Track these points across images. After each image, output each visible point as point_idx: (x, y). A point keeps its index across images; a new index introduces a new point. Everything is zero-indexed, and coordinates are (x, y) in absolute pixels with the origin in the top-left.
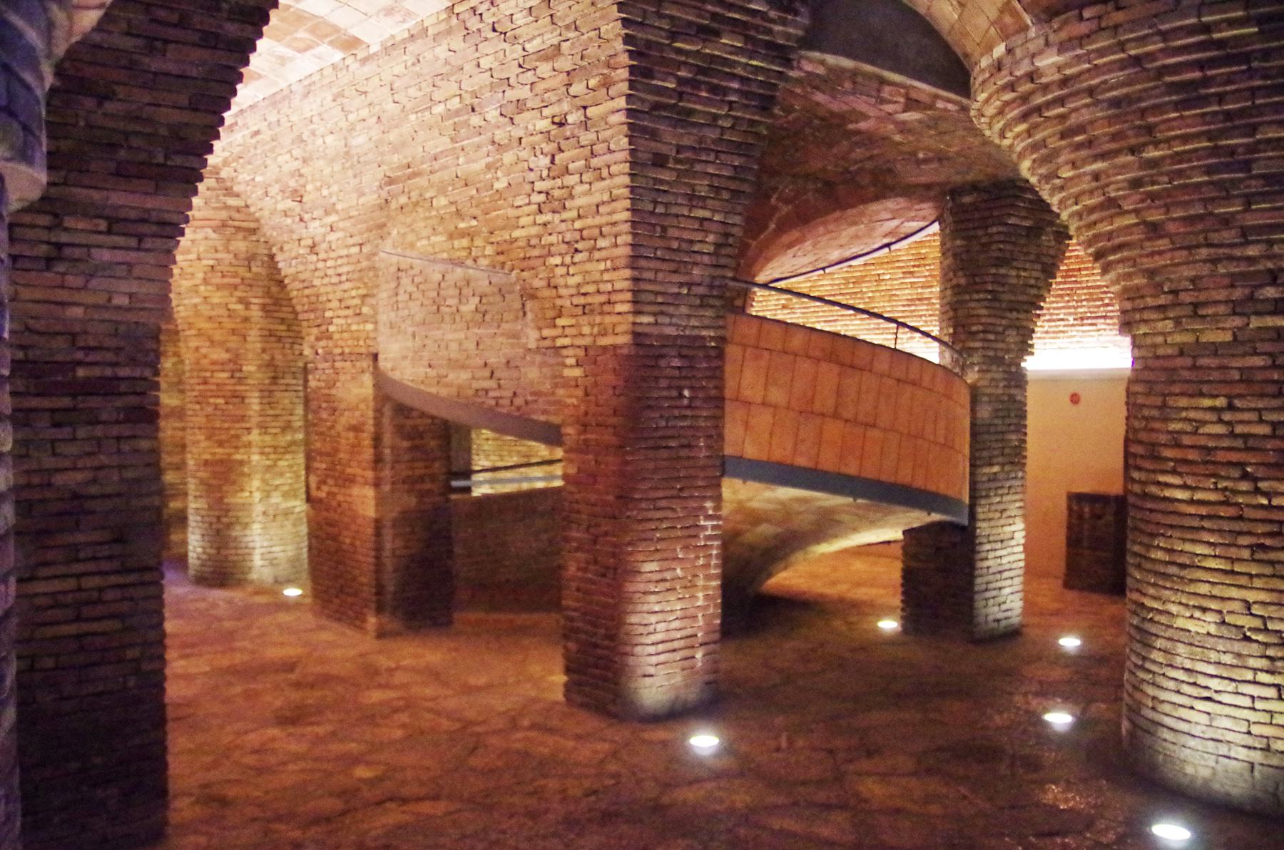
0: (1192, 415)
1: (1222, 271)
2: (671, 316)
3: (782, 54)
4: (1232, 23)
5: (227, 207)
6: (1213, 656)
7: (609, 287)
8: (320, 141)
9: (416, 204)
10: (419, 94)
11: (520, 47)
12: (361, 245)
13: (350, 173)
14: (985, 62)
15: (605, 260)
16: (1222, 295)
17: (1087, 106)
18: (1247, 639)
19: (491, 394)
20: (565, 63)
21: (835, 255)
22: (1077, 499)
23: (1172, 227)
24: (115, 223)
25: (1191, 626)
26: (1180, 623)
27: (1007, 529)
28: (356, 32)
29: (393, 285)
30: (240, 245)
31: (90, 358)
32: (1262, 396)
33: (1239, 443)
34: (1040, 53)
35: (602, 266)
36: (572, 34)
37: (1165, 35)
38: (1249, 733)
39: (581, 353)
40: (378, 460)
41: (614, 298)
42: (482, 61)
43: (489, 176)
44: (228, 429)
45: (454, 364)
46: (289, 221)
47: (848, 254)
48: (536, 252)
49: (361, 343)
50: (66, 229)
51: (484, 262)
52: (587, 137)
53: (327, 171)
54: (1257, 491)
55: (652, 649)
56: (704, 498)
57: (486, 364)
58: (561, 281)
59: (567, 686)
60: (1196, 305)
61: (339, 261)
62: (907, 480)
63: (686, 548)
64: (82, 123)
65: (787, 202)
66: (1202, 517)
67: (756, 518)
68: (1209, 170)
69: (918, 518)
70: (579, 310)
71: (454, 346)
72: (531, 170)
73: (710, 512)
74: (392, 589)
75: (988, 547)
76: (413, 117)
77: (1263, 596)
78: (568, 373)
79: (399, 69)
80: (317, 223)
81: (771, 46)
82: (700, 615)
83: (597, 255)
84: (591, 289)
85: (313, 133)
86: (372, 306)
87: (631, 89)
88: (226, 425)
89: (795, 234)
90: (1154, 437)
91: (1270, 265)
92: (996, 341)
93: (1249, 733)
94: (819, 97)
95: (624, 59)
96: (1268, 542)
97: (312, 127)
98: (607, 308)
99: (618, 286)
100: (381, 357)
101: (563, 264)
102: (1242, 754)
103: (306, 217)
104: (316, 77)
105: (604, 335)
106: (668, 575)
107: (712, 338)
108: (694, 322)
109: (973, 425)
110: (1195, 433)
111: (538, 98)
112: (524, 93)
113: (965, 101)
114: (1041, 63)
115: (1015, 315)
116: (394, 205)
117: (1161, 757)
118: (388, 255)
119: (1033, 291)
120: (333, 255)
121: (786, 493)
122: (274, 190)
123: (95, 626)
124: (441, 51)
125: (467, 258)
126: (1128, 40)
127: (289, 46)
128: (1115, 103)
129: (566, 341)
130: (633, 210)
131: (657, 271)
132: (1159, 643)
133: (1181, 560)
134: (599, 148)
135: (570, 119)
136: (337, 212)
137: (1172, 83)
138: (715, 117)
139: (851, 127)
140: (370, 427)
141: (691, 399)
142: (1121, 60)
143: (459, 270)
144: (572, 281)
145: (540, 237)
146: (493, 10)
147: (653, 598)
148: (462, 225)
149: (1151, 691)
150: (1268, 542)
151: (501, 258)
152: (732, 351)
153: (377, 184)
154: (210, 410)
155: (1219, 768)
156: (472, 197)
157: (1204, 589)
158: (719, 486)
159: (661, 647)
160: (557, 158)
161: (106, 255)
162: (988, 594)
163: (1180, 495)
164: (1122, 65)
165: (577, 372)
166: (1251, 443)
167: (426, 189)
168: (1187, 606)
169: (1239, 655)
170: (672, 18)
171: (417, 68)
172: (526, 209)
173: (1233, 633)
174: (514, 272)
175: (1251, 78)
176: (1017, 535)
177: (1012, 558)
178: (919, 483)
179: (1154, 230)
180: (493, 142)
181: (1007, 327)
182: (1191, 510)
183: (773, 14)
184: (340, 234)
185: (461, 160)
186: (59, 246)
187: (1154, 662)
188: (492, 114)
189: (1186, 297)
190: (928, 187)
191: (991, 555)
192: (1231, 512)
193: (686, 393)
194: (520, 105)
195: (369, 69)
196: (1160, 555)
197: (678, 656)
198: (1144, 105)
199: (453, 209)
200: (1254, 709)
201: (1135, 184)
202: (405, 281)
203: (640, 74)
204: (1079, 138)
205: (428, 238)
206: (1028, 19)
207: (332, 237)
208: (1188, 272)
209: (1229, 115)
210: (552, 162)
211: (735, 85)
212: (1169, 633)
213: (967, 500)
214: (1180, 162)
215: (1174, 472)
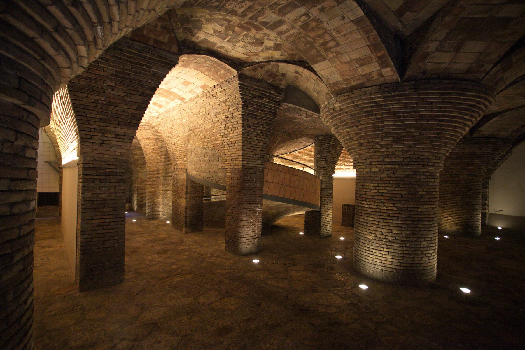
0: (370, 188)
1: (376, 154)
2: (251, 162)
3: (278, 104)
4: (378, 98)
5: (157, 136)
6: (374, 244)
8: (176, 121)
9: (196, 135)
10: (197, 110)
12: (184, 144)
13: (182, 128)
14: (323, 106)
15: (236, 148)
16: (376, 160)
17: (346, 116)
18: (381, 240)
19: (211, 179)
20: (228, 104)
21: (292, 150)
22: (345, 205)
23: (365, 144)
24: (117, 136)
25: (369, 237)
26: (366, 236)
27: (328, 212)
28: (183, 96)
29: (190, 153)
30: (160, 144)
31: (110, 167)
32: (385, 184)
33: (380, 195)
34: (335, 103)
36: (229, 97)
37: (363, 100)
38: (382, 263)
39: (231, 170)
40: (186, 193)
41: (239, 157)
42: (210, 103)
44: (156, 185)
45: (202, 171)
46: (169, 139)
47: (294, 150)
48: (221, 147)
50: (105, 137)
51: (210, 148)
52: (233, 121)
53: (177, 127)
54: (384, 206)
55: (245, 239)
56: (258, 204)
58: (227, 153)
60: (370, 162)
61: (180, 148)
62: (305, 201)
64: (110, 112)
65: (280, 137)
67: (271, 208)
68: (373, 131)
69: (308, 209)
70: (231, 160)
71: (203, 167)
74: (189, 222)
75: (324, 216)
76: (195, 116)
77: (385, 231)
78: (228, 174)
79: (192, 105)
80: (175, 139)
81: (275, 101)
83: (235, 147)
84: (233, 155)
85: (175, 119)
86: (186, 158)
87: (242, 109)
88: (155, 184)
89: (282, 145)
90: (361, 193)
91: (387, 153)
92: (326, 170)
93: (382, 263)
94: (287, 114)
95: (241, 103)
96: (387, 218)
98: (236, 160)
99: (239, 154)
101: (227, 149)
102: (380, 267)
103: (173, 138)
104: (175, 107)
106: (249, 222)
108: (256, 163)
109: (321, 189)
110: (370, 192)
111: (222, 112)
112: (219, 110)
113: (319, 115)
114: (335, 106)
115: (331, 164)
116: (191, 135)
117: (361, 268)
118: (190, 146)
119: (335, 159)
120: (178, 146)
122: (166, 132)
123: (108, 231)
124: (201, 101)
125: (206, 147)
126: (355, 101)
127: (169, 99)
128: (352, 115)
129: (228, 167)
130: (243, 137)
131: (248, 151)
132: (362, 241)
135: (229, 116)
137: (365, 111)
138: (262, 117)
139: (294, 121)
140: (185, 185)
141: (255, 181)
142: (354, 105)
143: (205, 150)
144: (229, 153)
145: (222, 143)
146: (212, 91)
147: (245, 227)
148: (206, 140)
149: (359, 252)
150: (387, 218)
151: (214, 148)
152: (266, 170)
154: (152, 180)
155: (375, 271)
157: (372, 228)
158: (262, 201)
159: (247, 238)
161: (115, 143)
162: (324, 227)
163: (367, 206)
164: (353, 107)
165: (230, 174)
166: (383, 194)
167: (198, 132)
169: (380, 244)
170: (252, 94)
171: (196, 105)
173: (379, 239)
175: (382, 110)
176: (331, 214)
177: (330, 219)
178: (308, 201)
179: (361, 144)
180: (213, 122)
181: (329, 167)
182: (369, 210)
183: (276, 94)
184: (180, 142)
185: (206, 125)
186: (103, 141)
187: (360, 245)
188: (212, 115)
189: (368, 161)
190: (312, 135)
191: (325, 218)
192: (378, 210)
193: (254, 179)
194: (218, 113)
195: (186, 105)
196: (362, 220)
198: (358, 116)
199: (204, 136)
200: (383, 257)
201: (357, 134)
202: (193, 152)
203: (245, 106)
204: (344, 123)
206: (332, 96)
207: (178, 142)
208: (368, 155)
209: (378, 119)
210: (225, 126)
211: (267, 110)
212: (364, 239)
214: (366, 129)
215: (365, 201)
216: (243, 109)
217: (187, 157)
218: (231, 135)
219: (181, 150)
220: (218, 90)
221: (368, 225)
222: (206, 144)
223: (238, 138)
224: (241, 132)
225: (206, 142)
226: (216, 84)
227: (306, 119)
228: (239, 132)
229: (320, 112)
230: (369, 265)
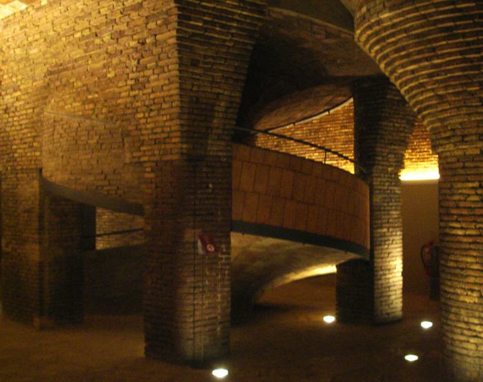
0: (464, 191)
1: (473, 119)
7: (168, 129)
8: (12, 52)
9: (65, 86)
10: (67, 27)
11: (121, 4)
13: (28, 69)
14: (358, 16)
15: (166, 115)
19: (105, 188)
25: (468, 300)
26: (462, 298)
29: (52, 130)
35: (165, 118)
40: (41, 229)
41: (171, 135)
42: (101, 11)
43: (105, 70)
47: (306, 115)
48: (130, 111)
49: (33, 163)
51: (101, 117)
52: (156, 50)
53: (16, 68)
56: (221, 243)
57: (102, 172)
59: (146, 349)
60: (464, 136)
61: (21, 118)
63: (211, 269)
66: (470, 243)
67: (253, 257)
71: (84, 162)
72: (127, 67)
73: (224, 250)
78: (147, 175)
79: (56, 14)
80: (9, 97)
82: (219, 307)
83: (162, 112)
84: (159, 130)
86: (39, 142)
87: (179, 25)
92: (383, 160)
95: (176, 11)
97: (8, 44)
98: (167, 140)
99: (173, 128)
100: (44, 170)
101: (144, 117)
104: (12, 18)
105: (166, 154)
107: (224, 157)
110: (465, 201)
111: (131, 30)
112: (123, 27)
113: (351, 33)
116: (52, 86)
117: (455, 369)
118: (49, 112)
119: (403, 134)
121: (268, 242)
126: (420, 7)
129: (146, 159)
130: (181, 89)
133: (461, 266)
134: (163, 56)
135: (148, 41)
136: (20, 90)
137: (441, 28)
138: (225, 41)
140: (37, 210)
141: (213, 189)
142: (418, 16)
144: (149, 126)
145: (132, 103)
148: (90, 97)
151: (111, 115)
153: (43, 75)
156: (95, 82)
158: (229, 236)
160: (141, 61)
162: (382, 299)
163: (460, 232)
165: (152, 175)
167: (71, 78)
168: (464, 289)
171: (67, 13)
172: (125, 88)
174: (118, 123)
180: (107, 53)
181: (388, 154)
184: (22, 102)
188: (107, 38)
193: (211, 186)
194: (121, 34)
195: (39, 14)
196: (452, 264)
197: (207, 329)
199: (85, 88)
202: (58, 128)
203: (183, 18)
204: (403, 53)
205: (71, 104)
207: (17, 104)
209: (468, 44)
210: (138, 63)
211: (235, 25)
213: (369, 247)
215: (457, 221)
216: (179, 23)
217: (40, 139)
218: (154, 84)
219: (24, 122)
221: (463, 272)
222: (91, 106)
223: (169, 90)
224: (177, 76)
225: (92, 101)
227: (327, 41)
228: (173, 76)
229: (353, 27)
230: (469, 360)
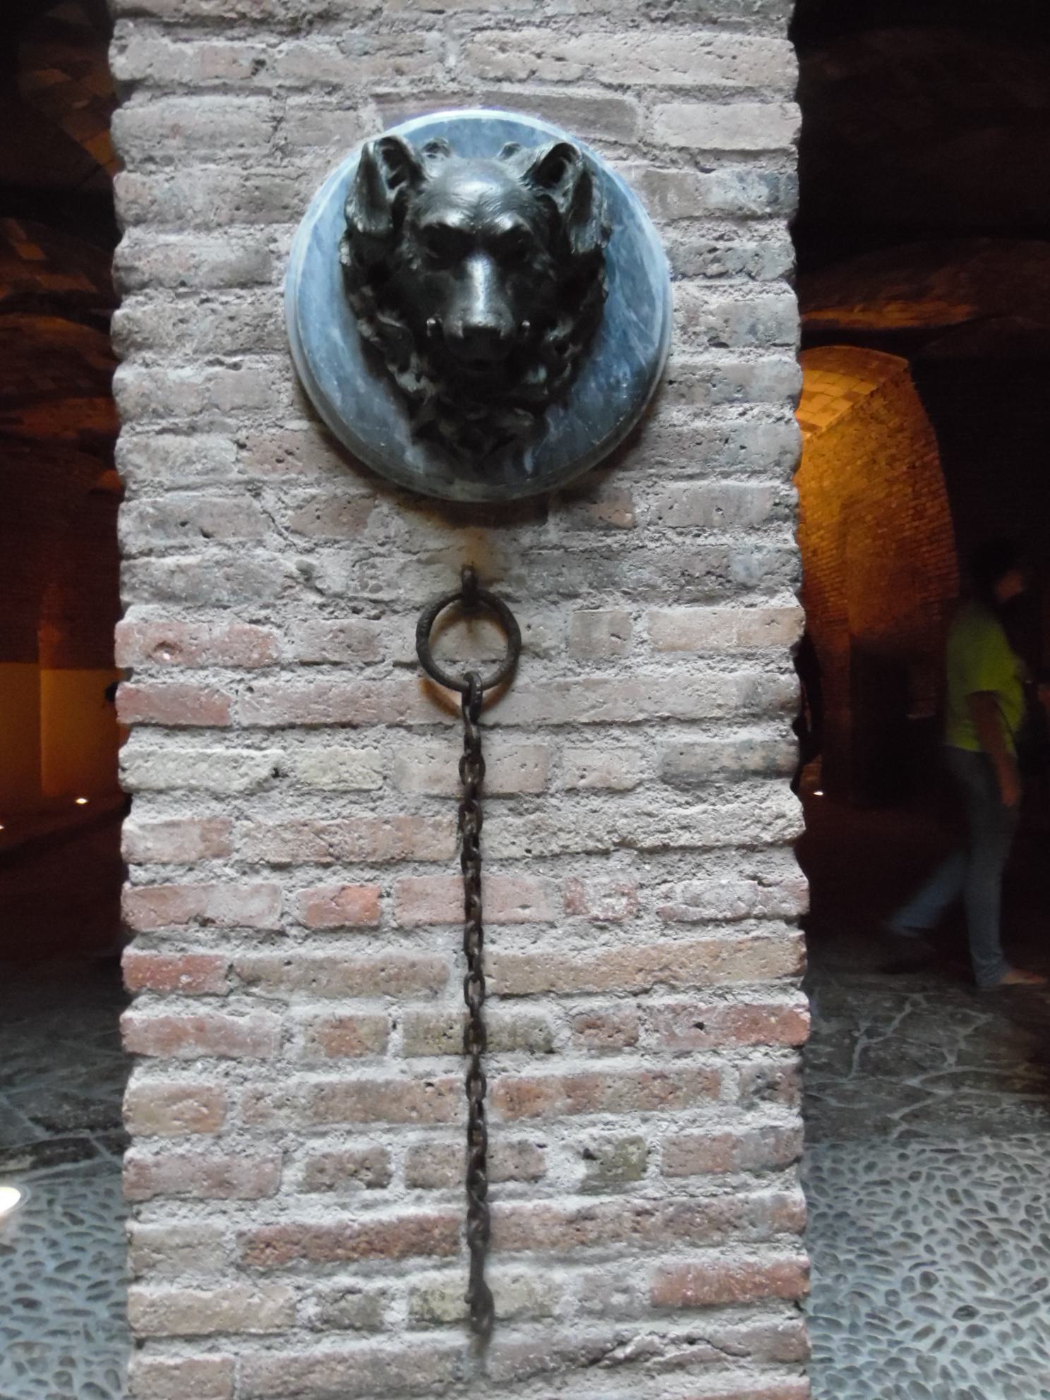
112: (893, 451)
207: (824, 544)
220: (878, 403)
226: (874, 388)
